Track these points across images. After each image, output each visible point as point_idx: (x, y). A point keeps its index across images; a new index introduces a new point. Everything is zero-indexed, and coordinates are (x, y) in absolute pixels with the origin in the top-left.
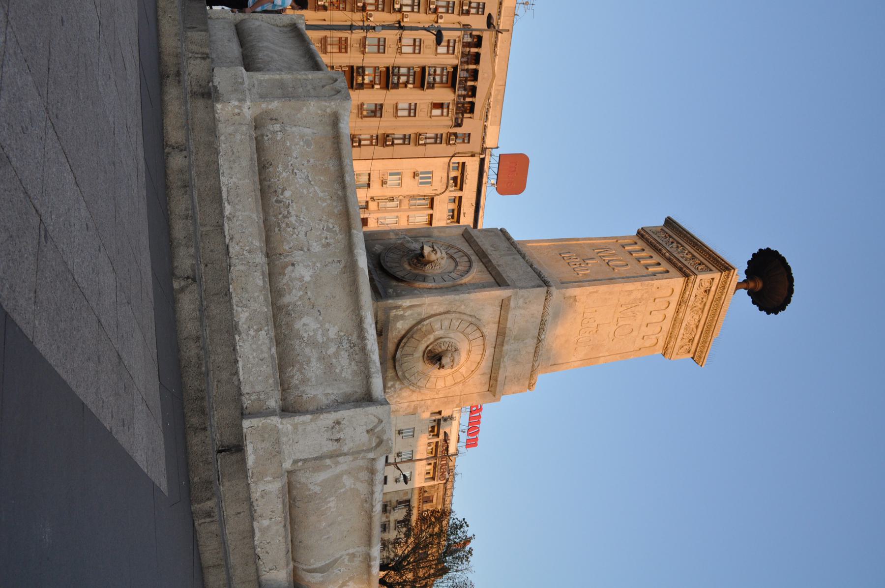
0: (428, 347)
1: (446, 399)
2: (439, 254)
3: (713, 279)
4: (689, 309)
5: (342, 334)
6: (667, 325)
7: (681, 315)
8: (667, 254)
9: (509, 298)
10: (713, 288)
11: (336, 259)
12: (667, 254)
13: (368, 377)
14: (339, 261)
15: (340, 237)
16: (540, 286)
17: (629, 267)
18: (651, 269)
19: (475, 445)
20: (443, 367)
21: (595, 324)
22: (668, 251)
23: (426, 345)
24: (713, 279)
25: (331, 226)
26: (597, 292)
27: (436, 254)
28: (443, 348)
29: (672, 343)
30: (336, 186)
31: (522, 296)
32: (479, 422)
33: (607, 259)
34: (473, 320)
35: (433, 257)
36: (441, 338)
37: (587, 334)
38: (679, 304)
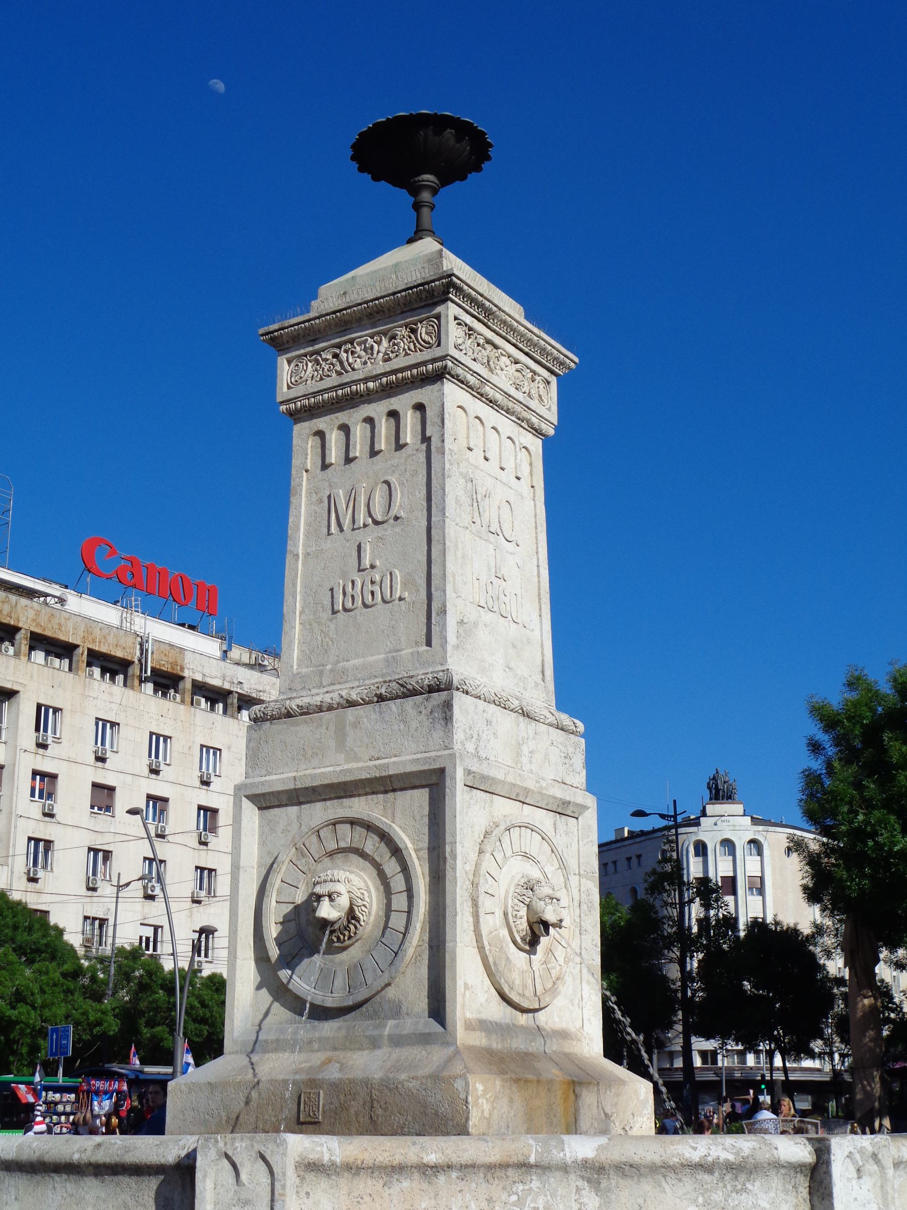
0: (515, 942)
1: (584, 907)
2: (341, 888)
3: (456, 318)
4: (494, 379)
5: (701, 1200)
6: (507, 425)
7: (499, 397)
8: (371, 385)
9: (469, 772)
10: (468, 320)
11: (574, 1197)
12: (371, 385)
13: (777, 1165)
14: (578, 1190)
15: (535, 1184)
16: (448, 706)
17: (393, 480)
18: (409, 435)
19: (212, 591)
20: (561, 921)
21: (495, 580)
22: (366, 380)
23: (512, 945)
24: (456, 318)
25: (514, 1198)
26: (454, 576)
27: (339, 894)
28: (523, 912)
29: (534, 420)
30: (442, 1178)
31: (463, 744)
32: (163, 573)
33: (362, 517)
34: (488, 848)
35: (344, 901)
36: (506, 914)
37: (507, 600)
38: (482, 396)
